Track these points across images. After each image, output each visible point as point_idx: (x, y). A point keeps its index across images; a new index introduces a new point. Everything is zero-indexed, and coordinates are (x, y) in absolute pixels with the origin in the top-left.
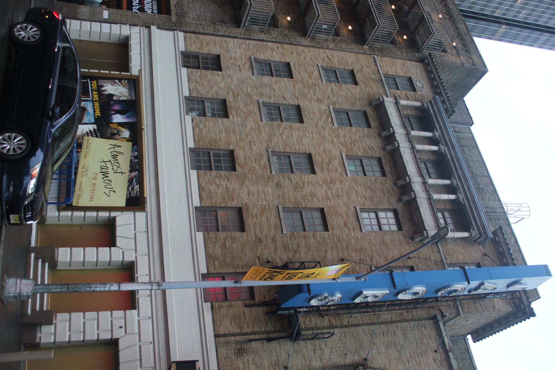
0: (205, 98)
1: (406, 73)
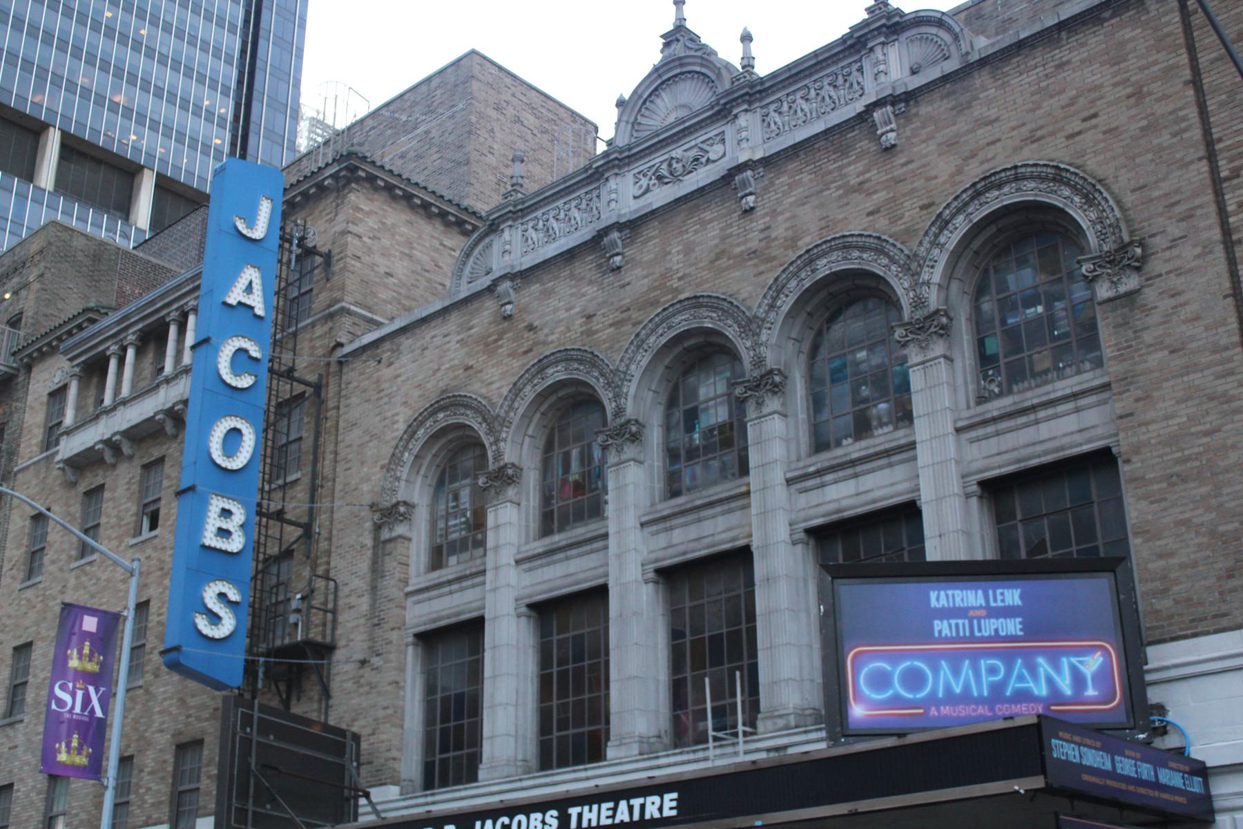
0: (45, 814)
1: (42, 404)
